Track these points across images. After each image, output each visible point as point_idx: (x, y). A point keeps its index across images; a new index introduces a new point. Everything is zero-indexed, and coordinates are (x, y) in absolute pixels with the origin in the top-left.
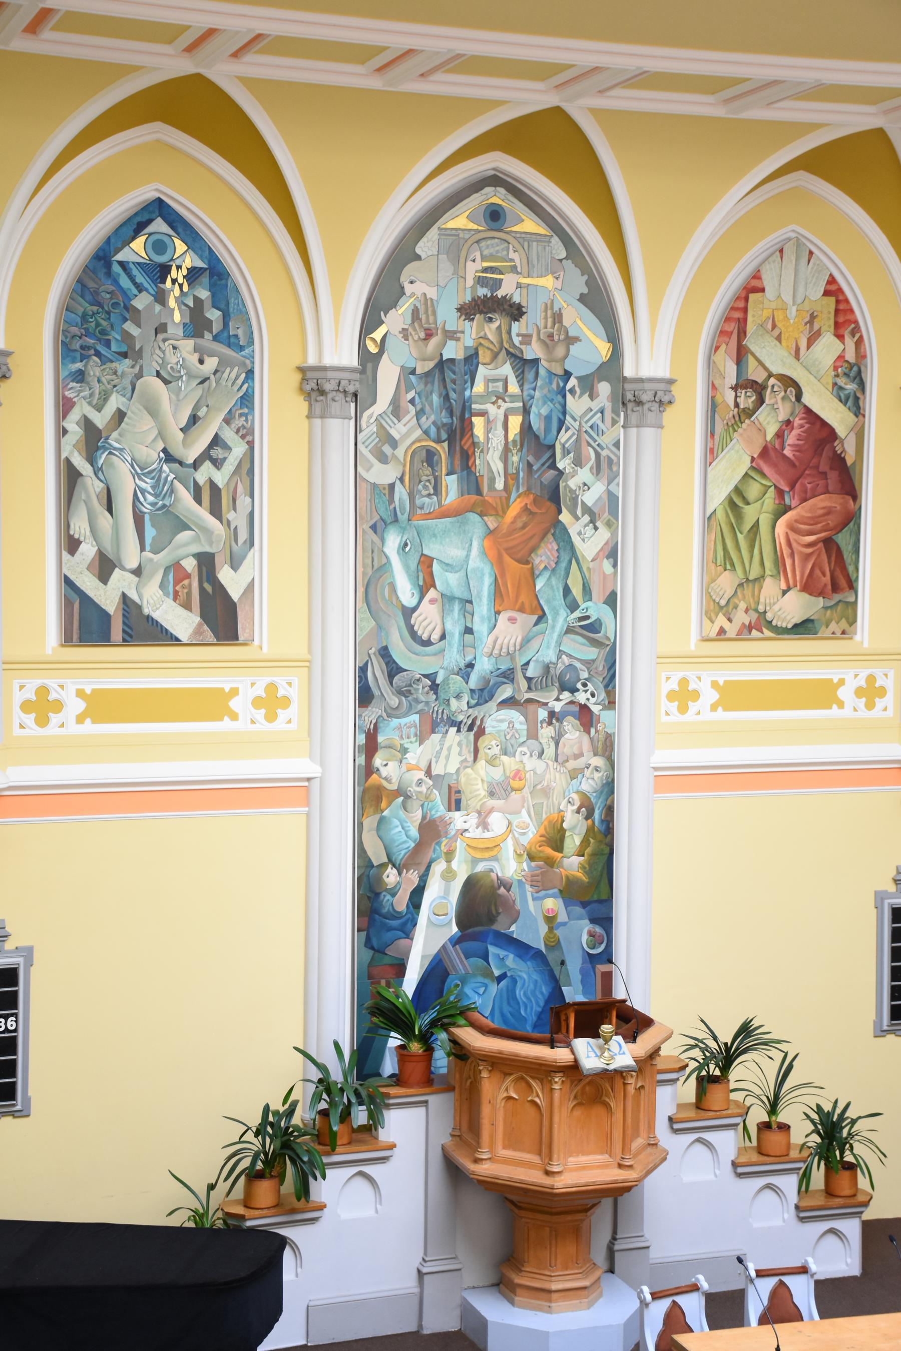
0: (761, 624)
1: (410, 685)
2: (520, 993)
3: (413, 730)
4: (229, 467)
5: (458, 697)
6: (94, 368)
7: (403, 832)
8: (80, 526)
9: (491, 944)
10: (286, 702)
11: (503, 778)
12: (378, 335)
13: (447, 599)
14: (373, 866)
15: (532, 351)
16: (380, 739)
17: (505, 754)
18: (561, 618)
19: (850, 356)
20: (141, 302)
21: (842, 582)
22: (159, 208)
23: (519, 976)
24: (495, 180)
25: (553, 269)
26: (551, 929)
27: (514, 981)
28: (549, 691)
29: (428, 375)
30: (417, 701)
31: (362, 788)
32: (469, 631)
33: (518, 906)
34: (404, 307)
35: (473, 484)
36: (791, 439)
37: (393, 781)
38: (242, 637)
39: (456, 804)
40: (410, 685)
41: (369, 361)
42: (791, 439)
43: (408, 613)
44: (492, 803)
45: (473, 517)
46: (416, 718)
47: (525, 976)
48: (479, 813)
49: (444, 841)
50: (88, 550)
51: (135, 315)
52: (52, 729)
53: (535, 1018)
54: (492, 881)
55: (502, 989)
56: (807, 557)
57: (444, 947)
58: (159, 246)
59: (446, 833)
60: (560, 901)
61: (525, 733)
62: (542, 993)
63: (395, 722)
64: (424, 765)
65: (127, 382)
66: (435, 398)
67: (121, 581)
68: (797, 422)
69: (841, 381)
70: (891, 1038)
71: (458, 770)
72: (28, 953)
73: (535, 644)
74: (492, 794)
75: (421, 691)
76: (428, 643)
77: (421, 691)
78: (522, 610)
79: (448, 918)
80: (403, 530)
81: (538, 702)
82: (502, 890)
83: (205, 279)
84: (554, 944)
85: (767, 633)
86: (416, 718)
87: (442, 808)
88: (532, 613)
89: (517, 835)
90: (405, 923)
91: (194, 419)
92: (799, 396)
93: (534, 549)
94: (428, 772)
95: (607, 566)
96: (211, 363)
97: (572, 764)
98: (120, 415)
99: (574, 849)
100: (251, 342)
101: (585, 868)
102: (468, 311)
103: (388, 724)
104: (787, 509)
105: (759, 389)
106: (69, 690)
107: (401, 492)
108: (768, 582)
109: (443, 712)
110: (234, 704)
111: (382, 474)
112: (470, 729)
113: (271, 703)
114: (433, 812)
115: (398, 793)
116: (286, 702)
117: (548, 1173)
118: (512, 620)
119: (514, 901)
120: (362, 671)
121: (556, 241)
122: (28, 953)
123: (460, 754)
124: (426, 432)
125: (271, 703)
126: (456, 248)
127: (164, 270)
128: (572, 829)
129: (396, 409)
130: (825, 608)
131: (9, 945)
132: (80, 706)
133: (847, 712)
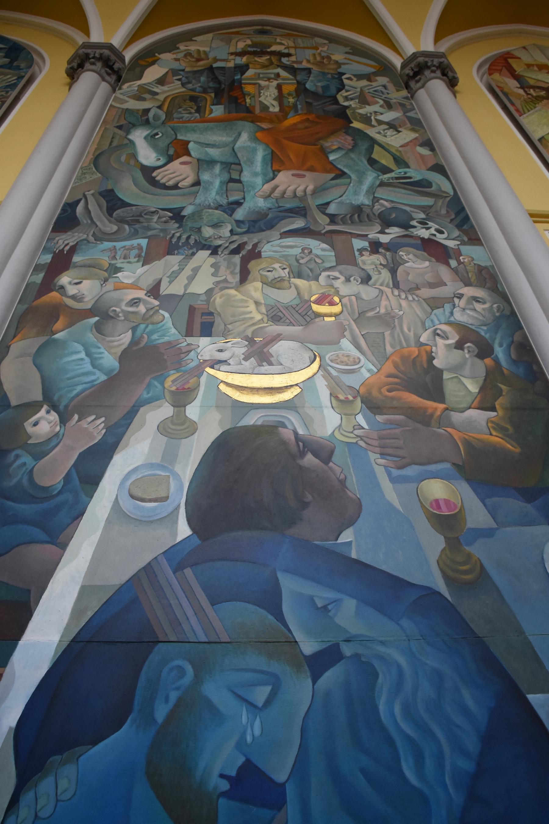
1: (141, 216)
2: (389, 709)
7: (87, 360)
9: (287, 571)
11: (297, 301)
14: (8, 406)
17: (299, 276)
23: (382, 658)
26: (454, 544)
27: (368, 673)
31: (25, 307)
37: (86, 299)
40: (141, 216)
44: (274, 329)
47: (401, 660)
48: (251, 341)
49: (173, 375)
54: (284, 443)
57: (148, 570)
59: (178, 365)
61: (334, 258)
63: (107, 245)
71: (210, 292)
81: (350, 233)
82: (310, 460)
86: (144, 242)
87: (173, 331)
88: (329, 172)
89: (334, 373)
94: (154, 291)
97: (426, 293)
99: (469, 399)
101: (506, 430)
109: (188, 238)
114: (155, 337)
119: (343, 483)
128: (456, 369)
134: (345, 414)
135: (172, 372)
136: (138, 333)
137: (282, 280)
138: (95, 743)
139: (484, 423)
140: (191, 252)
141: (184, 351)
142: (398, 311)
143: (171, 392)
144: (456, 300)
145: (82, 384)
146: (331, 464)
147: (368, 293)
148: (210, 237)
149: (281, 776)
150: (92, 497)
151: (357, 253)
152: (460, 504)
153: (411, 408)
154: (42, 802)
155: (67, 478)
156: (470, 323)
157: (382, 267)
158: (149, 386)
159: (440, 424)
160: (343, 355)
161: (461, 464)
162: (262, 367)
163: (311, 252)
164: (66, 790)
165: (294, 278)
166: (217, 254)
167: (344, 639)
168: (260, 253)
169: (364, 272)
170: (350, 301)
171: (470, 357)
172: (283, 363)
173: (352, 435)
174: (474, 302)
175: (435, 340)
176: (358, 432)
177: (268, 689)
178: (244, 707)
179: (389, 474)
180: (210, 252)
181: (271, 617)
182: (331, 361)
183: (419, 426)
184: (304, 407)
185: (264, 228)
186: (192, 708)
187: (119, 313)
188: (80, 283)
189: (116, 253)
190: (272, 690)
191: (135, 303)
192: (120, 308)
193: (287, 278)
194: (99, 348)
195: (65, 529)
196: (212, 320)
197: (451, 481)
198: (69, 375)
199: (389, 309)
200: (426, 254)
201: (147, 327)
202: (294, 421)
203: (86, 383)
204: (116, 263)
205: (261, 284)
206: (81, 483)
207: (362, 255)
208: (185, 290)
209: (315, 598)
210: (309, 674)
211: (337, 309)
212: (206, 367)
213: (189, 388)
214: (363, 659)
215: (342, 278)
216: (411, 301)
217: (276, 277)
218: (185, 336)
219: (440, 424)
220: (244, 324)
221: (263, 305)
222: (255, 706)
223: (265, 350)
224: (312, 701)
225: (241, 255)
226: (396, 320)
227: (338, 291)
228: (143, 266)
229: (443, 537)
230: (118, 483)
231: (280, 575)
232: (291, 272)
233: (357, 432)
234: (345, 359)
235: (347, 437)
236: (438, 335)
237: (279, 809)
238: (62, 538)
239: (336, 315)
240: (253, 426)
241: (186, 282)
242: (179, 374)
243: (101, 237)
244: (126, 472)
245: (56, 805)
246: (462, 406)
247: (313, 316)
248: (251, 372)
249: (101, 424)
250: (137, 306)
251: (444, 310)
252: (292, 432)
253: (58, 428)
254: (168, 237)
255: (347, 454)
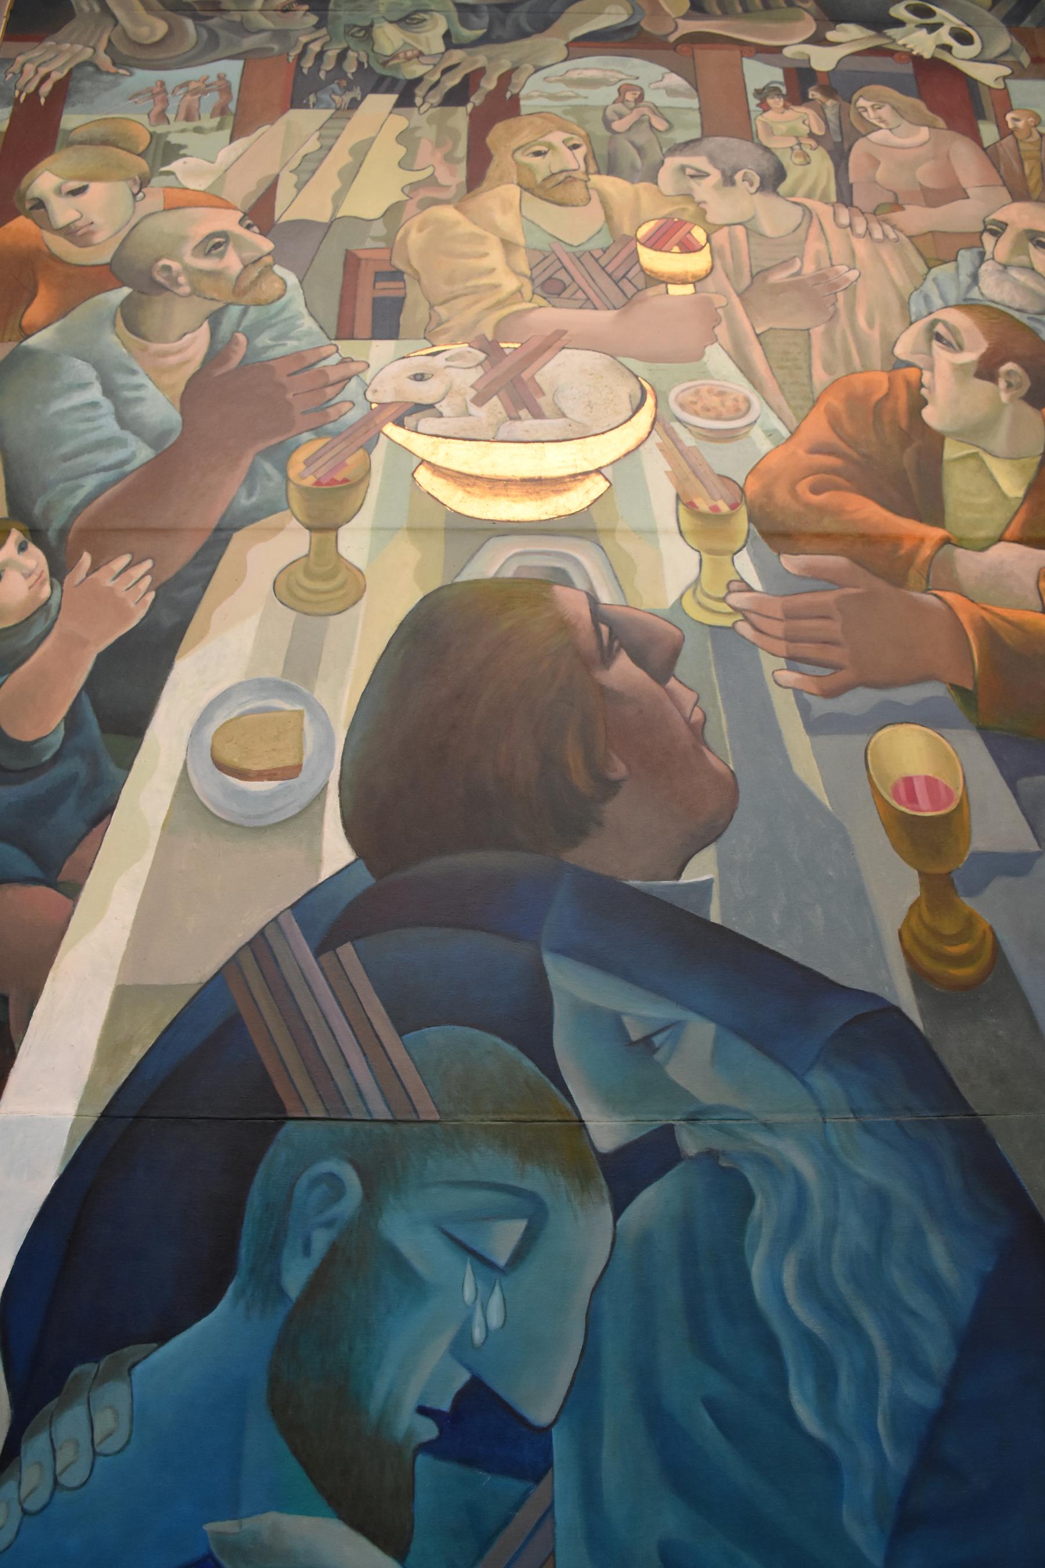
2: (772, 1274)
3: (212, 99)
7: (107, 405)
9: (564, 951)
11: (604, 240)
17: (611, 168)
23: (766, 1162)
26: (939, 890)
28: (782, 20)
30: (243, 29)
33: (724, 749)
37: (98, 238)
44: (550, 316)
46: (232, 70)
47: (805, 1166)
48: (491, 349)
49: (309, 446)
53: (898, 1461)
54: (564, 625)
55: (645, 1239)
57: (260, 946)
60: (974, 744)
61: (696, 117)
62: (931, 1282)
63: (145, 78)
64: (243, 190)
71: (393, 214)
79: (302, 789)
82: (623, 671)
86: (232, 70)
87: (308, 323)
89: (688, 439)
90: (45, 805)
94: (260, 213)
97: (917, 218)
99: (1000, 516)
103: (115, 84)
109: (342, 56)
112: (456, 97)
114: (263, 340)
119: (698, 730)
123: (405, 164)
128: (975, 432)
134: (711, 552)
135: (306, 436)
136: (226, 327)
137: (567, 178)
138: (162, 1338)
139: (1030, 581)
140: (347, 97)
141: (333, 376)
142: (845, 268)
143: (305, 491)
144: (988, 240)
145: (98, 471)
146: (672, 683)
147: (776, 216)
148: (394, 56)
149: (542, 1412)
150: (129, 767)
151: (753, 102)
152: (960, 792)
153: (863, 536)
154: (65, 1456)
155: (73, 720)
156: (1017, 306)
157: (813, 143)
158: (251, 477)
159: (928, 581)
160: (709, 391)
161: (970, 688)
162: (517, 423)
163: (641, 98)
164: (110, 1435)
165: (599, 173)
166: (412, 104)
167: (684, 1117)
168: (516, 98)
169: (768, 156)
170: (732, 238)
171: (1011, 400)
172: (566, 411)
173: (723, 607)
174: (1031, 246)
175: (930, 352)
176: (738, 599)
177: (521, 1225)
178: (469, 1267)
179: (804, 709)
180: (393, 98)
181: (528, 1063)
182: (682, 406)
183: (880, 585)
184: (612, 531)
185: (528, 28)
186: (359, 1264)
187: (179, 274)
188: (82, 190)
189: (166, 101)
190: (527, 1229)
191: (216, 246)
192: (179, 259)
193: (579, 175)
194: (134, 372)
195: (73, 850)
196: (399, 294)
197: (944, 731)
198: (66, 448)
199: (825, 263)
200: (921, 105)
201: (245, 312)
202: (587, 563)
203: (105, 469)
204: (169, 133)
205: (518, 189)
206: (104, 730)
207: (765, 107)
208: (336, 208)
209: (626, 1019)
210: (606, 1194)
211: (698, 262)
212: (384, 423)
213: (345, 480)
214: (724, 1163)
215: (716, 176)
216: (879, 241)
217: (555, 170)
218: (337, 339)
219: (928, 581)
220: (476, 302)
221: (523, 251)
222: (491, 1265)
223: (526, 375)
224: (611, 1255)
225: (470, 106)
226: (841, 296)
227: (704, 212)
228: (231, 140)
229: (916, 872)
230: (187, 730)
231: (551, 963)
232: (592, 155)
233: (736, 599)
234: (715, 401)
235: (714, 612)
236: (939, 337)
237: (538, 1479)
238: (66, 873)
239: (697, 280)
240: (494, 580)
241: (338, 185)
242: (321, 443)
243: (130, 55)
244: (203, 703)
245: (93, 1464)
246: (982, 534)
247: (640, 282)
248: (490, 435)
249: (143, 577)
250: (221, 256)
251: (957, 268)
252: (585, 596)
253: (46, 590)
254: (293, 54)
255: (711, 657)
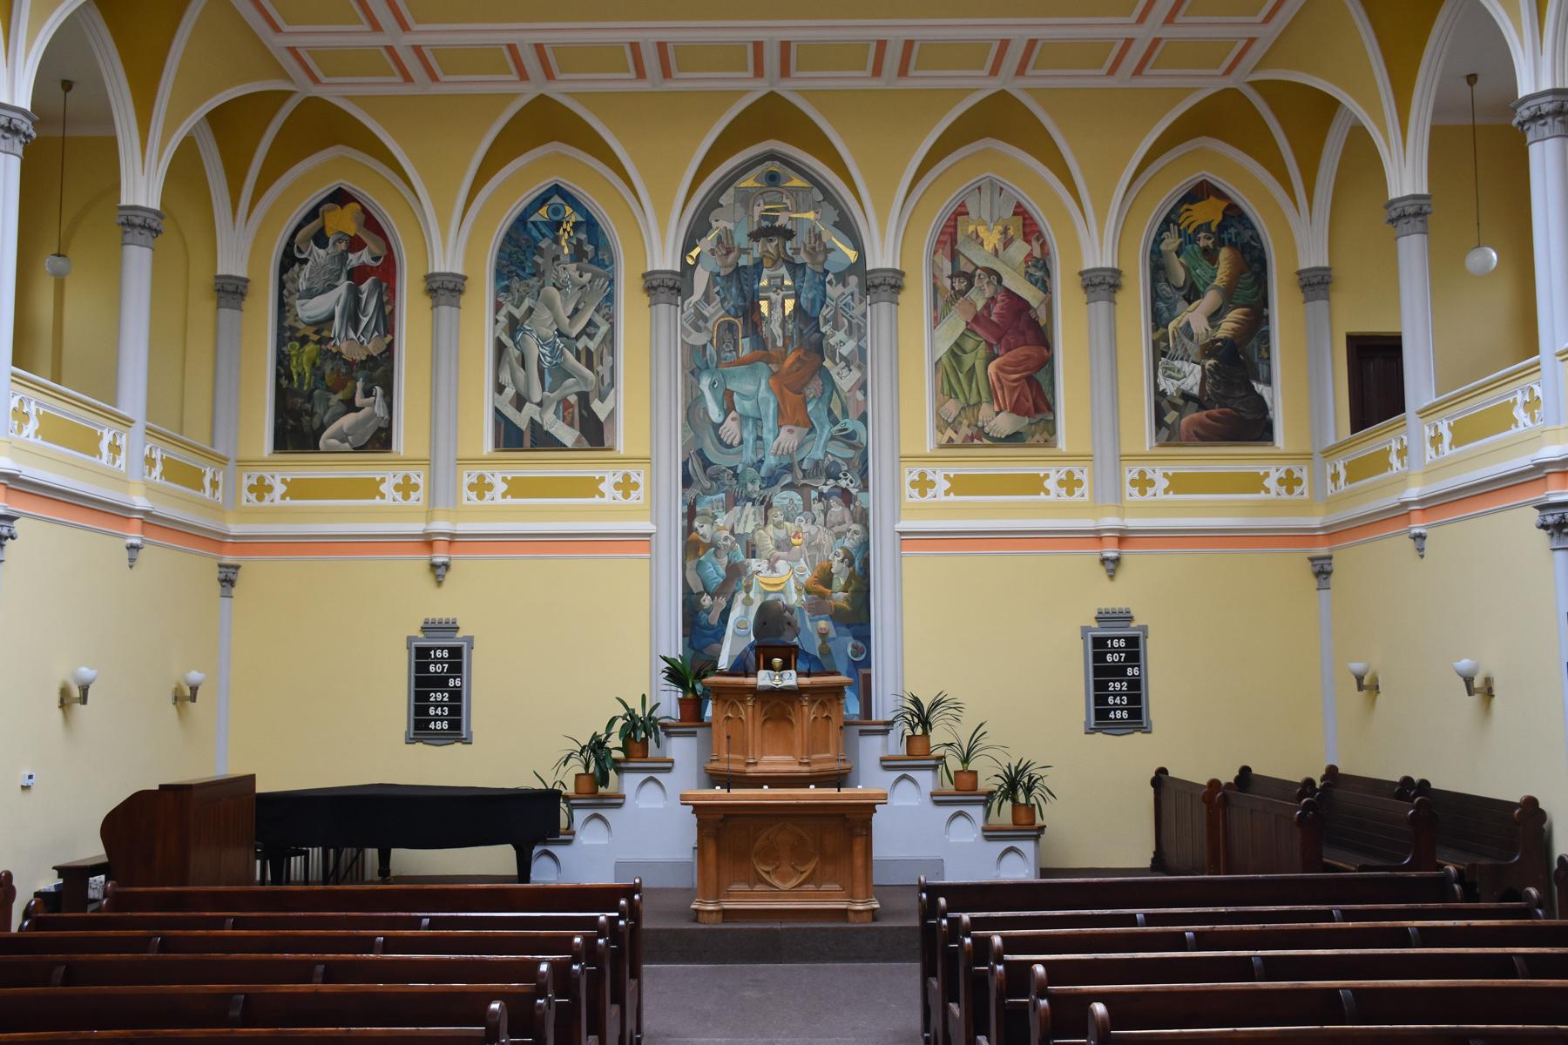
0: (980, 436)
4: (598, 338)
5: (753, 482)
6: (515, 283)
8: (505, 377)
10: (636, 486)
12: (694, 253)
13: (743, 419)
15: (802, 258)
16: (698, 509)
18: (827, 430)
19: (1037, 253)
20: (543, 244)
21: (1043, 406)
22: (557, 189)
24: (772, 156)
25: (815, 207)
26: (824, 642)
29: (728, 277)
32: (759, 438)
33: (799, 625)
34: (712, 236)
35: (760, 342)
36: (996, 309)
38: (607, 445)
39: (752, 552)
41: (687, 271)
42: (996, 309)
43: (717, 427)
44: (778, 553)
45: (761, 364)
50: (510, 391)
51: (540, 252)
52: (486, 501)
56: (1013, 389)
58: (556, 211)
64: (729, 527)
65: (535, 290)
66: (733, 290)
67: (530, 410)
68: (999, 298)
69: (1031, 270)
70: (1099, 735)
72: (470, 640)
73: (808, 447)
74: (778, 548)
75: (726, 477)
76: (731, 446)
77: (726, 477)
78: (797, 425)
80: (712, 374)
83: (584, 228)
84: (826, 652)
85: (986, 442)
91: (576, 310)
92: (1000, 280)
93: (805, 385)
94: (732, 532)
95: (859, 395)
96: (587, 276)
97: (836, 529)
98: (531, 310)
100: (612, 263)
102: (755, 236)
104: (995, 357)
105: (970, 278)
106: (497, 480)
107: (711, 350)
108: (984, 406)
110: (602, 487)
111: (698, 339)
113: (626, 486)
115: (711, 545)
116: (636, 486)
117: (748, 764)
118: (791, 431)
120: (685, 464)
121: (816, 191)
122: (470, 640)
124: (728, 312)
125: (626, 486)
126: (746, 199)
127: (559, 224)
128: (839, 573)
129: (707, 297)
130: (1030, 424)
131: (459, 635)
132: (504, 487)
133: (1052, 497)
147: (813, 529)
